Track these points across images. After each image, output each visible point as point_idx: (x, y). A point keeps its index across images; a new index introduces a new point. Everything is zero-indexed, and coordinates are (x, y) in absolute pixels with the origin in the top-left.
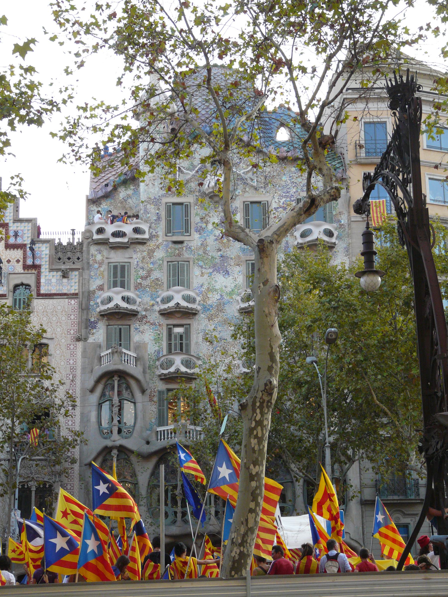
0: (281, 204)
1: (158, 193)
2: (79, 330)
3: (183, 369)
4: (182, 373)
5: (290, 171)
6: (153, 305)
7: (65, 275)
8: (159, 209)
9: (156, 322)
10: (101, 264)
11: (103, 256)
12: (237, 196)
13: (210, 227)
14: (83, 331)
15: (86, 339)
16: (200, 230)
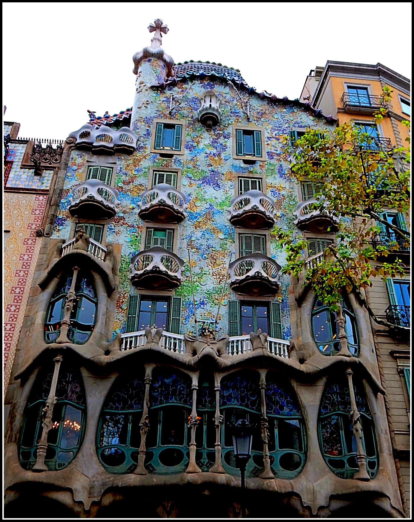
0: (274, 135)
1: (150, 114)
2: (43, 225)
3: (163, 268)
4: (160, 272)
5: (281, 112)
6: (133, 209)
7: (38, 173)
8: (149, 127)
9: (135, 224)
10: (80, 167)
11: (84, 160)
12: (229, 124)
13: (201, 146)
14: (47, 227)
15: (49, 234)
16: (190, 148)
